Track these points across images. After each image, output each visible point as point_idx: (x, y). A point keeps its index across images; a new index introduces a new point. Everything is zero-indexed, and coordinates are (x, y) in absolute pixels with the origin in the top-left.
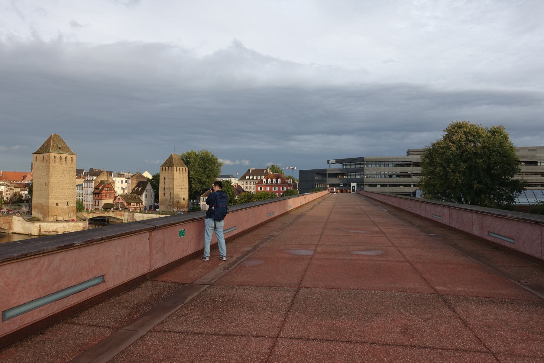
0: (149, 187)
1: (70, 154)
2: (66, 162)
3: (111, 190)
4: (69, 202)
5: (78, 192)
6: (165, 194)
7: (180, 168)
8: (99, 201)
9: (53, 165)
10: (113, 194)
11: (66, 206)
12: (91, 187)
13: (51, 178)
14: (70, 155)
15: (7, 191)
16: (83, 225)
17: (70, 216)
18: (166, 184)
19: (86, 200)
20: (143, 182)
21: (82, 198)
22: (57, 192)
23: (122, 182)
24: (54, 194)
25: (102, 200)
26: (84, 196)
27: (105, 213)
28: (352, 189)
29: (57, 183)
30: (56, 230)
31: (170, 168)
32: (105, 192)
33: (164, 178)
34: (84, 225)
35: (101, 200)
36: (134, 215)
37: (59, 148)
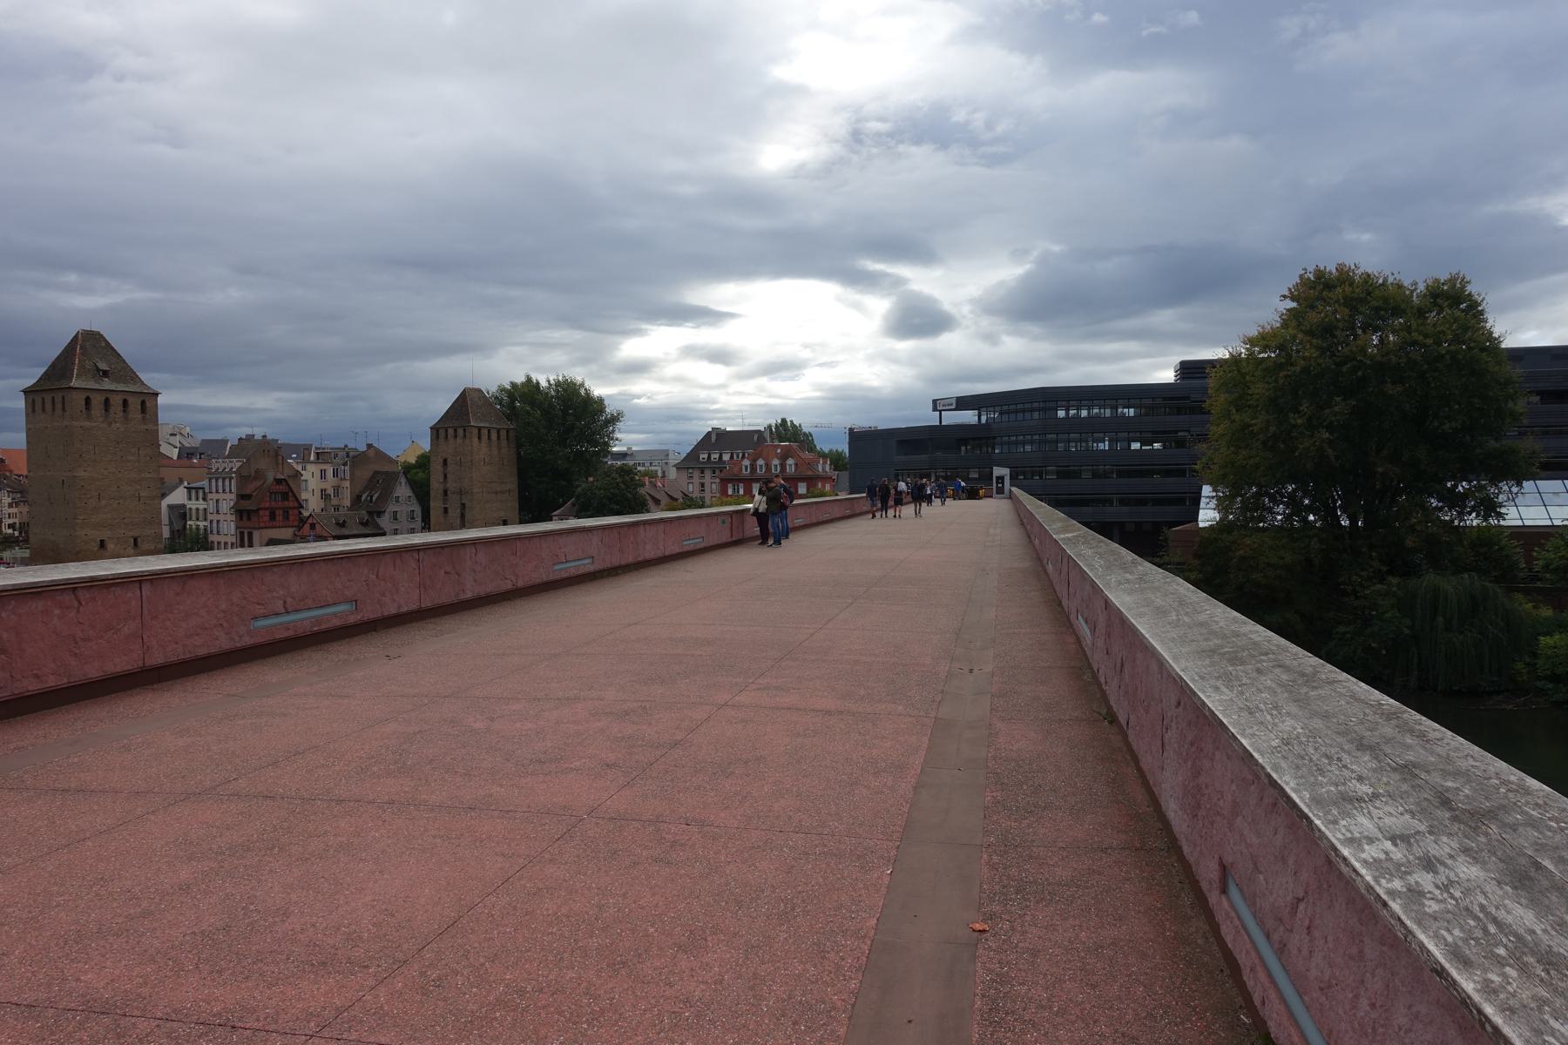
0: (403, 490)
2: (126, 419)
3: (288, 500)
5: (194, 507)
8: (250, 535)
9: (83, 424)
10: (296, 511)
12: (227, 490)
15: (10, 505)
19: (215, 531)
20: (387, 473)
21: (205, 524)
23: (323, 474)
26: (210, 517)
28: (995, 485)
31: (460, 432)
32: (267, 505)
33: (442, 460)
37: (101, 374)
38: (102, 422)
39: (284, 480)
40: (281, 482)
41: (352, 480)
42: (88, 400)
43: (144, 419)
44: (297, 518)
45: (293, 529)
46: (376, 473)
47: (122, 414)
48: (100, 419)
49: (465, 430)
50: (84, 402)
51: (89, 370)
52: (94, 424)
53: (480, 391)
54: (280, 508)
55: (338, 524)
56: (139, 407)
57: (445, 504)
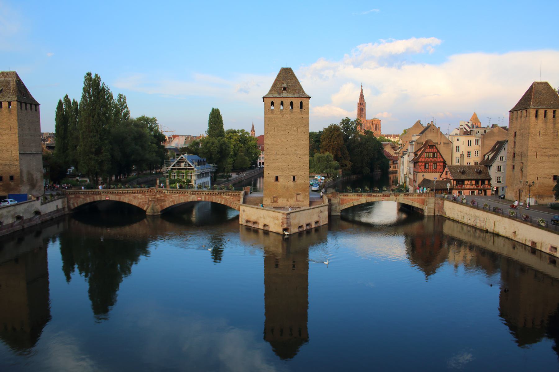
1: (299, 96)
2: (291, 112)
4: (296, 176)
6: (514, 165)
7: (546, 112)
8: (416, 174)
9: (269, 116)
11: (291, 183)
13: (267, 138)
14: (299, 98)
16: (282, 218)
17: (298, 199)
18: (516, 146)
22: (276, 159)
23: (469, 143)
24: (272, 163)
25: (419, 173)
27: (389, 197)
32: (423, 160)
33: (513, 133)
34: (283, 218)
35: (418, 172)
36: (443, 203)
37: (283, 89)
41: (483, 146)
43: (301, 112)
44: (442, 168)
45: (441, 174)
46: (498, 142)
49: (526, 111)
51: (278, 88)
52: (275, 116)
53: (546, 83)
54: (431, 162)
57: (514, 163)
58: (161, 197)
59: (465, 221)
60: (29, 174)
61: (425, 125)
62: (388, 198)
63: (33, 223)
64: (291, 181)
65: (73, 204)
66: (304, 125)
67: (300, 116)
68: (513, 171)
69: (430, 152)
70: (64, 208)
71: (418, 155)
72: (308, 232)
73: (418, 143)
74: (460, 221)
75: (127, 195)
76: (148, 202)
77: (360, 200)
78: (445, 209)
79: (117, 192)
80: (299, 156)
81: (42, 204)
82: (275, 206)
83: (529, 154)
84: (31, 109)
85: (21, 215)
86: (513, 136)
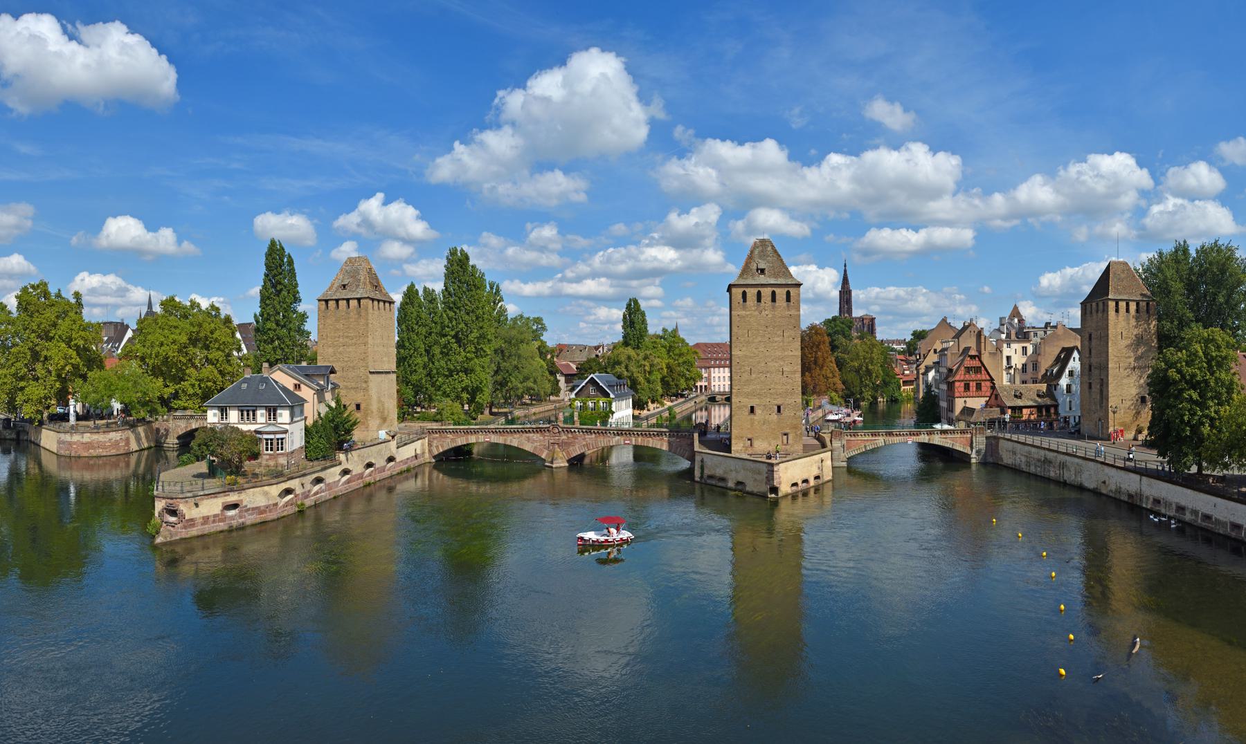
2: (774, 307)
6: (1090, 384)
8: (952, 401)
11: (774, 417)
13: (736, 347)
24: (745, 385)
29: (751, 357)
30: (725, 476)
31: (1101, 304)
32: (962, 378)
36: (998, 443)
37: (759, 271)
38: (755, 311)
39: (977, 356)
40: (975, 359)
42: (744, 294)
43: (788, 305)
46: (1064, 349)
47: (770, 303)
48: (753, 308)
50: (741, 296)
52: (748, 313)
55: (1016, 396)
56: (785, 297)
58: (568, 438)
59: (1032, 470)
60: (380, 401)
61: (959, 326)
62: (918, 437)
63: (387, 474)
64: (774, 414)
65: (437, 447)
66: (792, 327)
67: (787, 313)
68: (1090, 392)
69: (972, 365)
70: (423, 453)
71: (954, 370)
72: (805, 494)
73: (952, 354)
74: (1024, 470)
75: (517, 436)
76: (547, 445)
77: (877, 441)
78: (1000, 451)
79: (501, 430)
80: (785, 376)
81: (397, 448)
82: (750, 453)
83: (1110, 366)
84: (385, 309)
85: (373, 462)
86: (1088, 339)
